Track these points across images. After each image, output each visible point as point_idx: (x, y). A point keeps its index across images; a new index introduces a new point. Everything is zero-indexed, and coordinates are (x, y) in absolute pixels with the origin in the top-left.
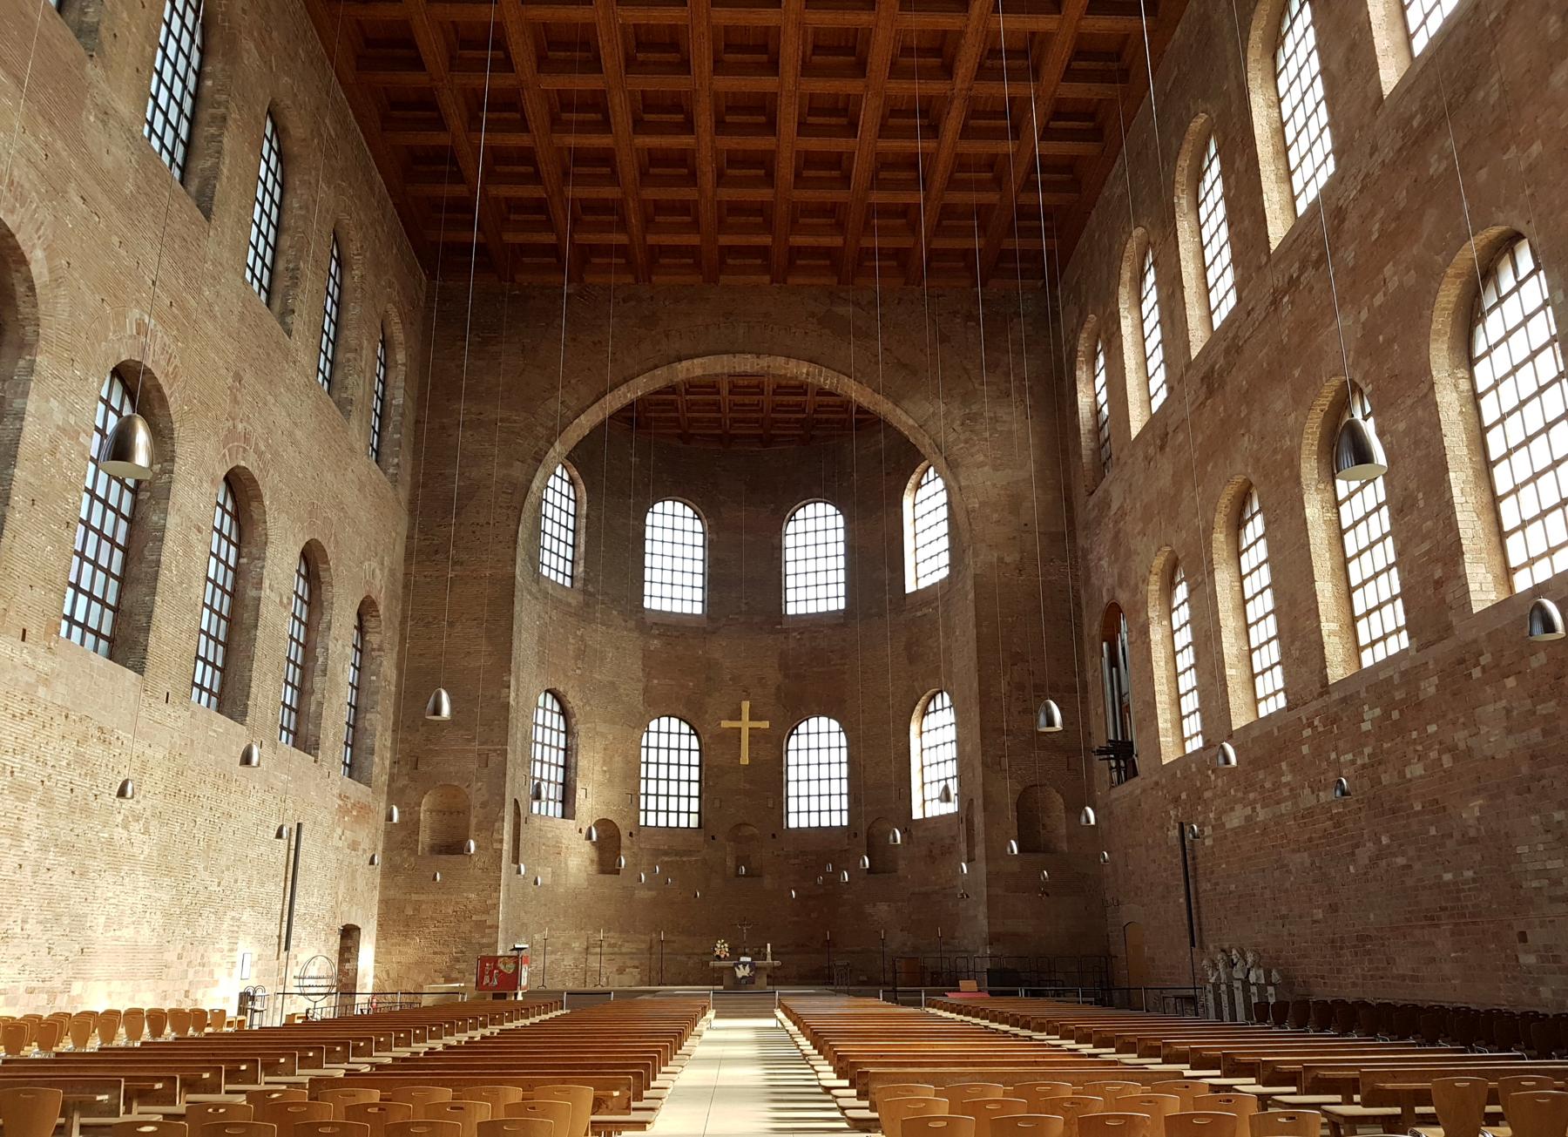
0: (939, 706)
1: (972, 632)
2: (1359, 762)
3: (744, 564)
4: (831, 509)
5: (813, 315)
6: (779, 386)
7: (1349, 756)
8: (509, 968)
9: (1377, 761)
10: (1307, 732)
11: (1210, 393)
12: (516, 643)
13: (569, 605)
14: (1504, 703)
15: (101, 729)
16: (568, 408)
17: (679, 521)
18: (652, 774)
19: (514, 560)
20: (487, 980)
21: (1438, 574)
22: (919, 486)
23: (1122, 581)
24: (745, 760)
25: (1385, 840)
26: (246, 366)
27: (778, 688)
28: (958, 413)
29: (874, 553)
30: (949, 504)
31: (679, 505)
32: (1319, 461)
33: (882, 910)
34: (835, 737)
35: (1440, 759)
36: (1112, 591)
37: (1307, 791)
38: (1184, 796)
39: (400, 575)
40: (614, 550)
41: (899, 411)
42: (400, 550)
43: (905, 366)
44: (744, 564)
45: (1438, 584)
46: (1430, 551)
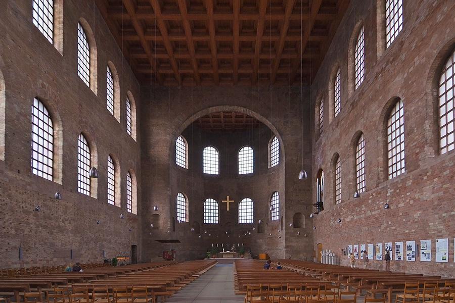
3: (228, 162)
4: (250, 148)
6: (237, 116)
14: (433, 185)
15: (50, 198)
17: (212, 152)
18: (207, 211)
23: (323, 162)
24: (228, 209)
26: (83, 102)
30: (280, 146)
31: (212, 148)
34: (250, 203)
36: (320, 165)
40: (196, 158)
41: (267, 121)
44: (228, 162)
45: (417, 154)
46: (415, 145)
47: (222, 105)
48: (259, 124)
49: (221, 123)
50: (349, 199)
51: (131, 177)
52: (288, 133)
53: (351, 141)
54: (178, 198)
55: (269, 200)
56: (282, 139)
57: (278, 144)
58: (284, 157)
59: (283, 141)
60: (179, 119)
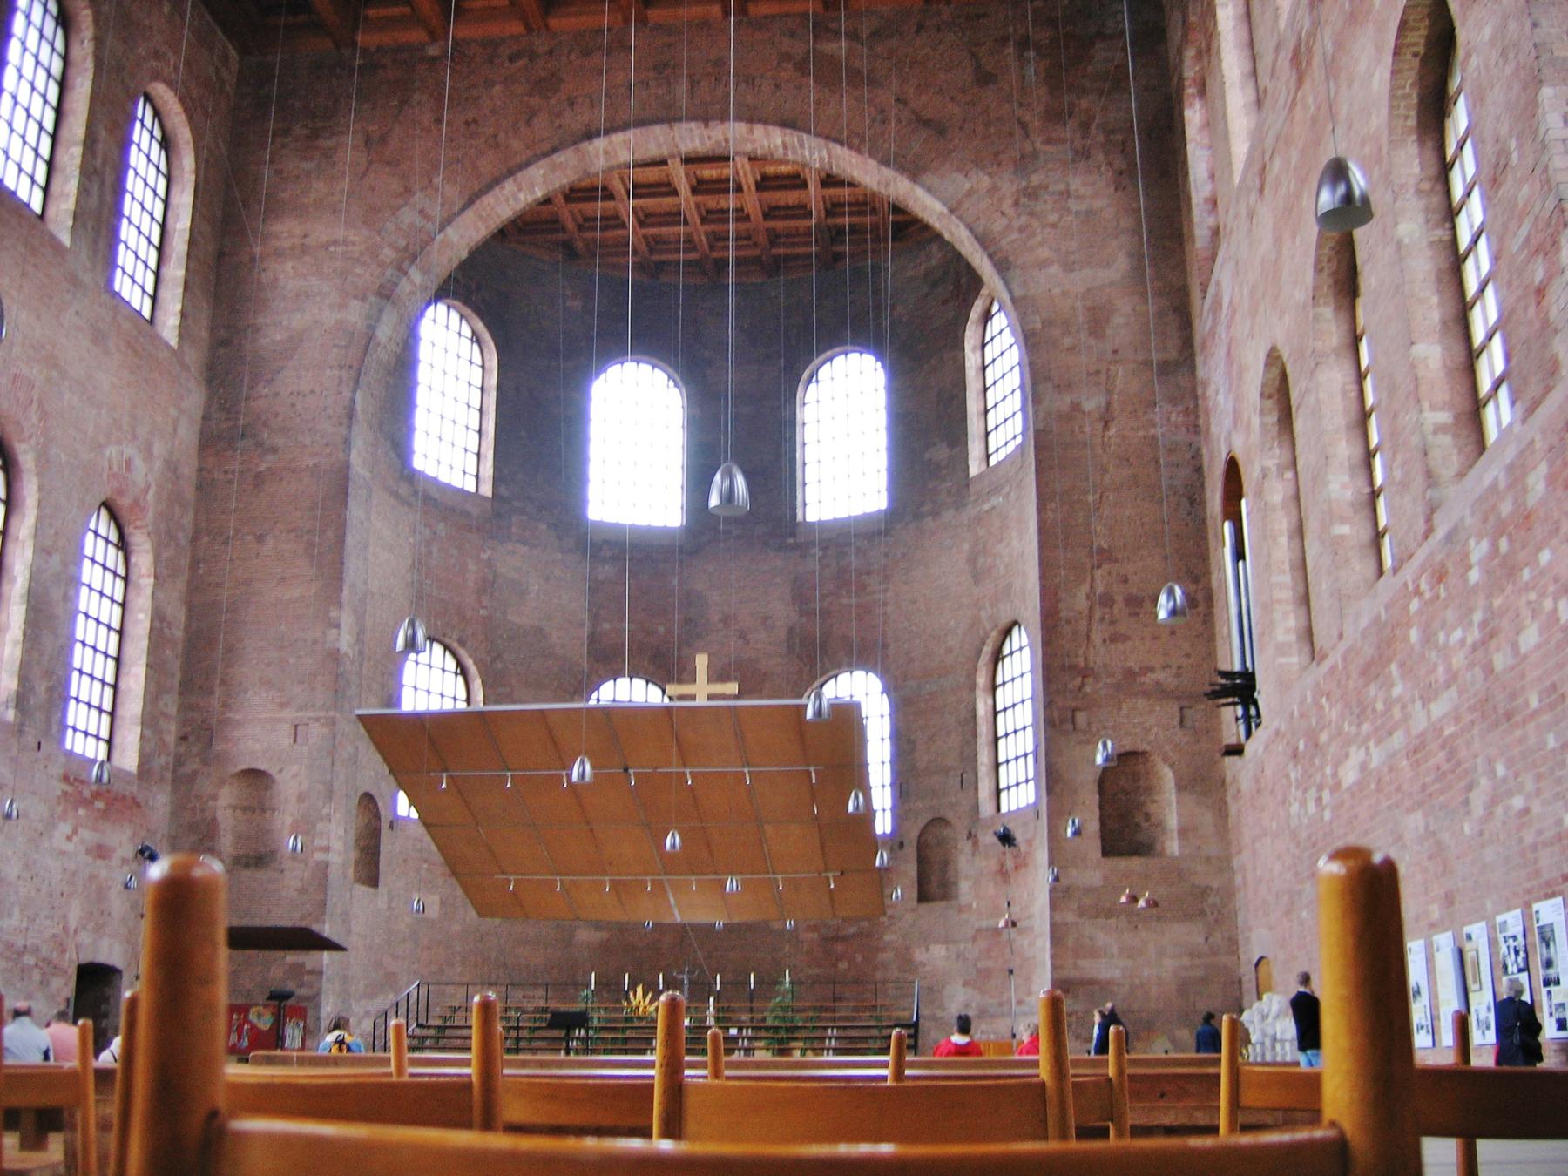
0: (1016, 646)
2: (1469, 641)
5: (787, 57)
6: (765, 177)
7: (1457, 634)
9: (1490, 633)
10: (1415, 605)
11: (1300, 81)
13: (468, 515)
16: (428, 218)
19: (347, 442)
21: (1539, 275)
22: (987, 316)
25: (1500, 770)
27: (791, 631)
28: (1008, 186)
29: (929, 421)
32: (1421, 142)
33: (935, 956)
35: (1555, 610)
37: (1418, 705)
39: (188, 470)
41: (919, 192)
43: (927, 123)
46: (1527, 239)
50: (1341, 636)
52: (1044, 253)
53: (1318, 270)
55: (982, 680)
56: (1010, 292)
59: (1013, 300)
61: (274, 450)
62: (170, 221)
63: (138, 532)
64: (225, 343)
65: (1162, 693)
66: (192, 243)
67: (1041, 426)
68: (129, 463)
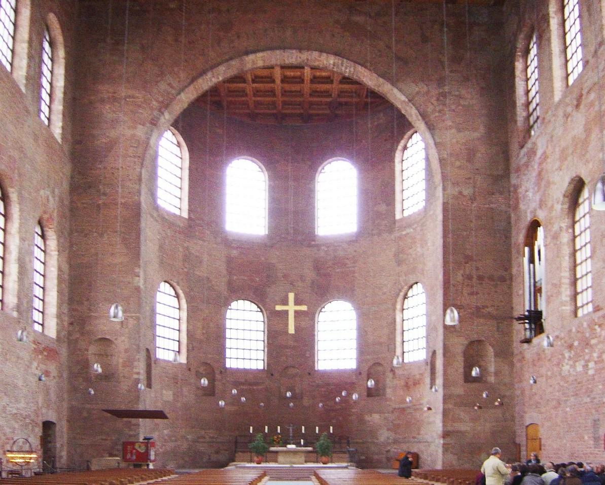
1: (439, 242)
6: (315, 77)
8: (142, 450)
12: (143, 248)
19: (139, 192)
20: (129, 456)
30: (427, 159)
38: (576, 343)
40: (204, 185)
42: (66, 185)
47: (279, 48)
48: (378, 101)
49: (274, 95)
51: (43, 236)
54: (160, 297)
57: (423, 154)
58: (440, 188)
60: (169, 84)
61: (105, 194)
62: (54, 82)
63: (50, 230)
64: (79, 142)
65: (490, 316)
66: (65, 93)
67: (445, 201)
68: (48, 197)
